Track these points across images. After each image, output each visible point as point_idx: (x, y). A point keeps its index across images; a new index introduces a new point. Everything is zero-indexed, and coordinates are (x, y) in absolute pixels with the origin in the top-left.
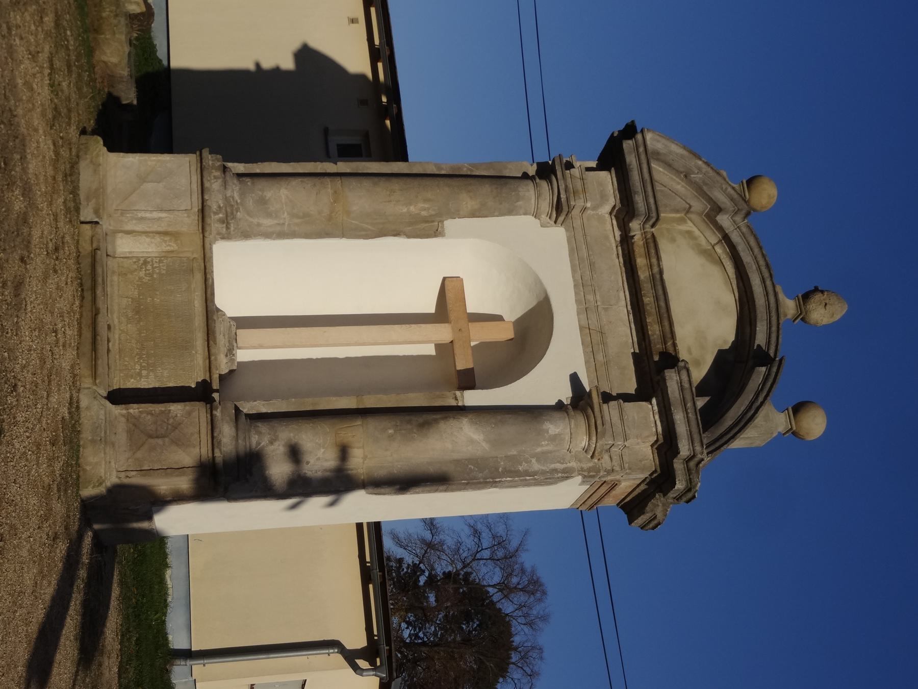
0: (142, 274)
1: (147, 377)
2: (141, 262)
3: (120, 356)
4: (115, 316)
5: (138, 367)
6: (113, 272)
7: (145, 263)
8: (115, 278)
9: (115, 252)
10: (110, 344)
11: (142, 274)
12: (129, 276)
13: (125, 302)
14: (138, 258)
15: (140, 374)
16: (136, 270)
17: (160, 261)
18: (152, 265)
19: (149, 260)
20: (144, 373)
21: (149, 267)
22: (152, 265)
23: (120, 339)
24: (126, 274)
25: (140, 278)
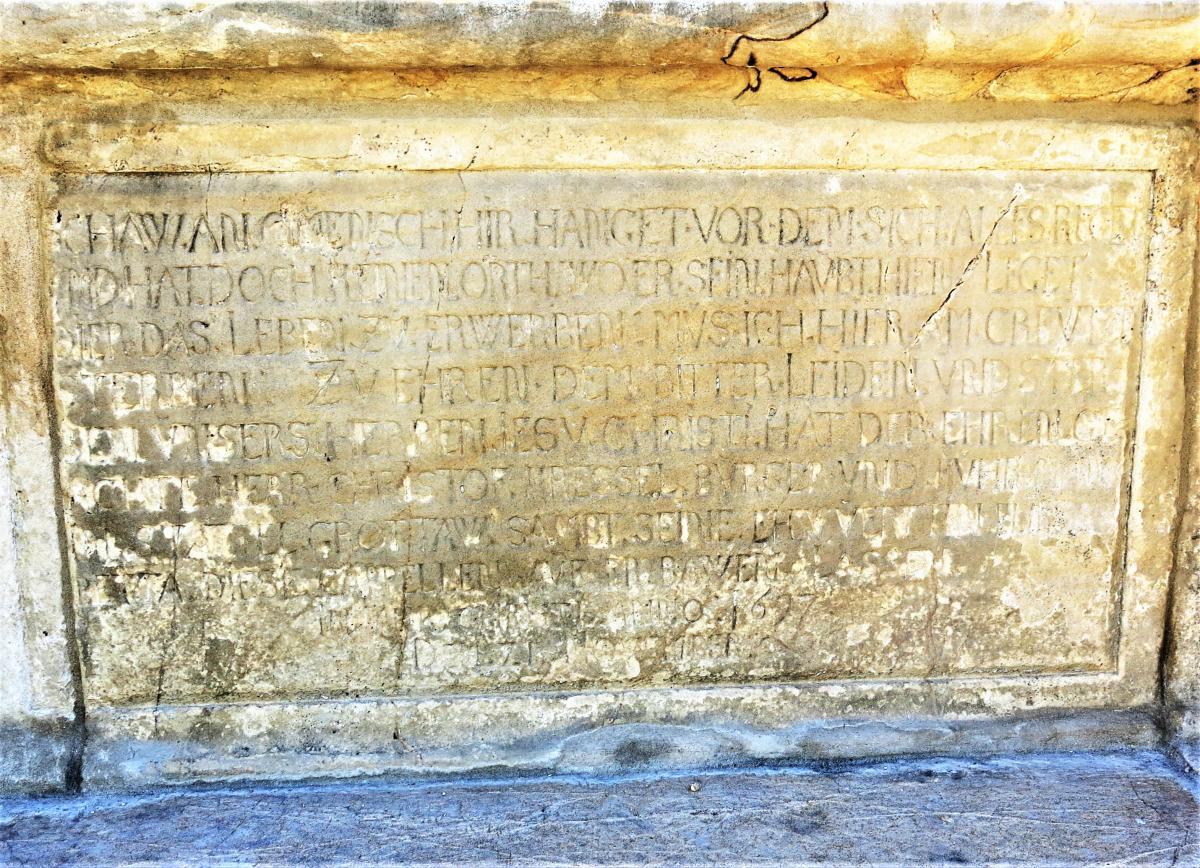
0: (208, 544)
1: (992, 506)
2: (108, 550)
3: (831, 674)
4: (538, 714)
5: (919, 564)
6: (205, 732)
7: (110, 520)
8: (251, 719)
9: (44, 728)
10: (762, 745)
11: (208, 544)
12: (226, 628)
13: (437, 655)
14: (75, 573)
15: (970, 553)
16: (172, 585)
17: (94, 413)
18: (131, 472)
19: (86, 496)
20: (962, 523)
21: (149, 494)
22: (131, 472)
23: (713, 678)
24: (216, 652)
25: (245, 552)
